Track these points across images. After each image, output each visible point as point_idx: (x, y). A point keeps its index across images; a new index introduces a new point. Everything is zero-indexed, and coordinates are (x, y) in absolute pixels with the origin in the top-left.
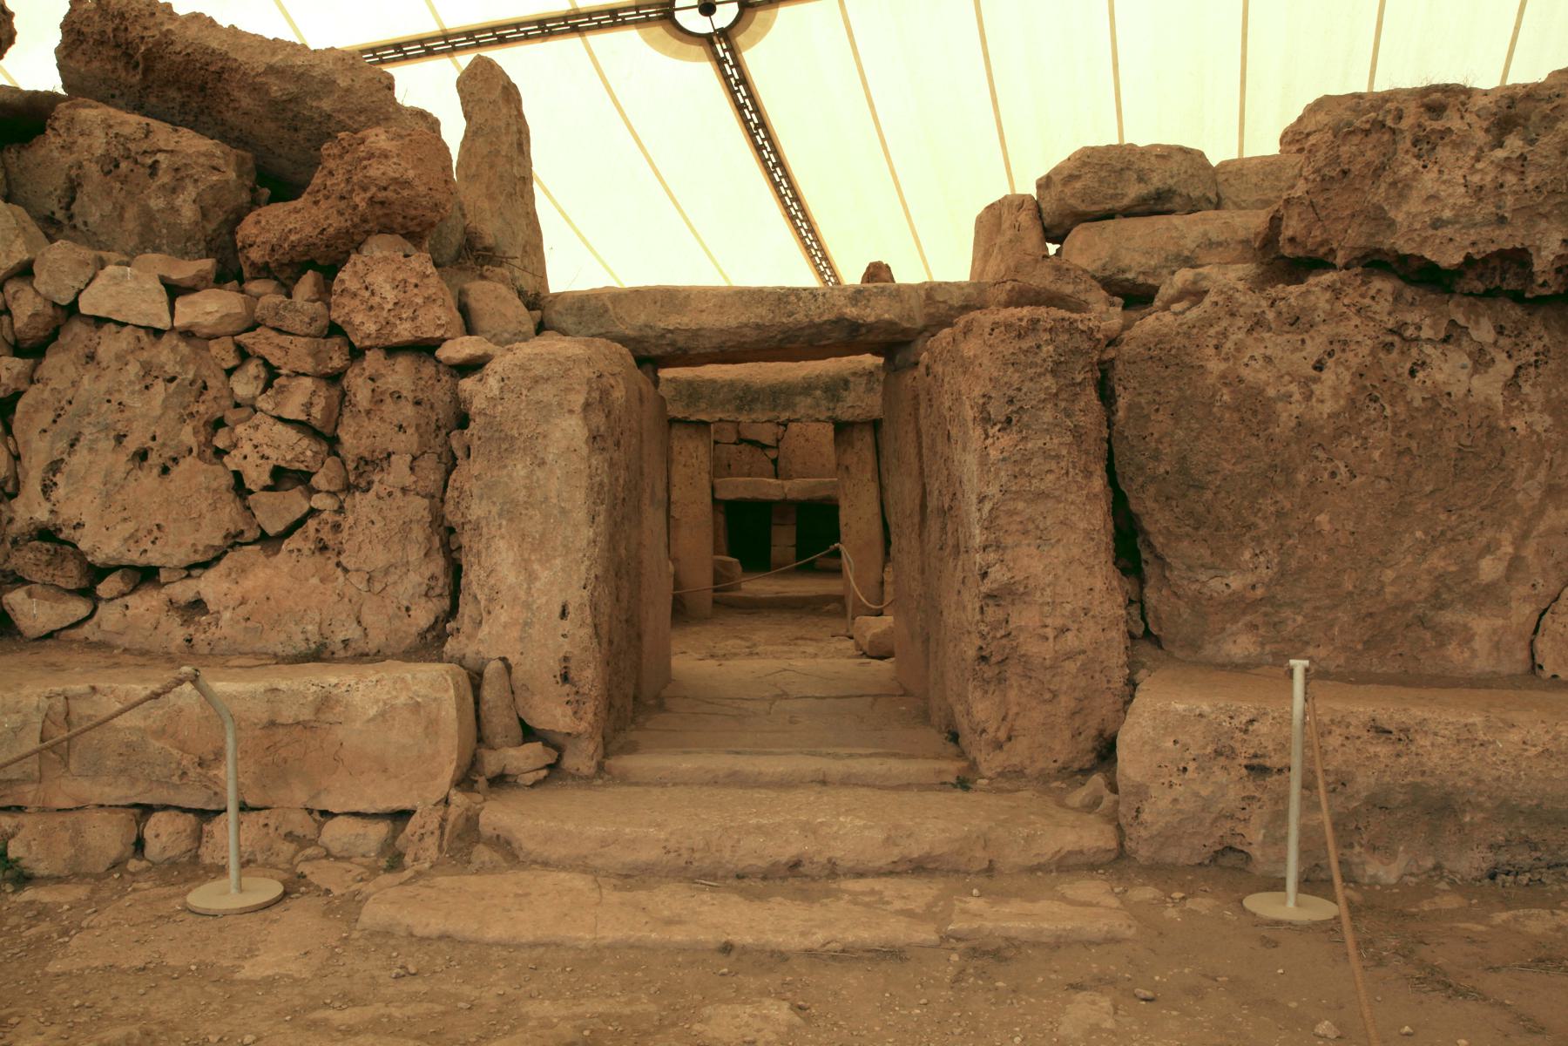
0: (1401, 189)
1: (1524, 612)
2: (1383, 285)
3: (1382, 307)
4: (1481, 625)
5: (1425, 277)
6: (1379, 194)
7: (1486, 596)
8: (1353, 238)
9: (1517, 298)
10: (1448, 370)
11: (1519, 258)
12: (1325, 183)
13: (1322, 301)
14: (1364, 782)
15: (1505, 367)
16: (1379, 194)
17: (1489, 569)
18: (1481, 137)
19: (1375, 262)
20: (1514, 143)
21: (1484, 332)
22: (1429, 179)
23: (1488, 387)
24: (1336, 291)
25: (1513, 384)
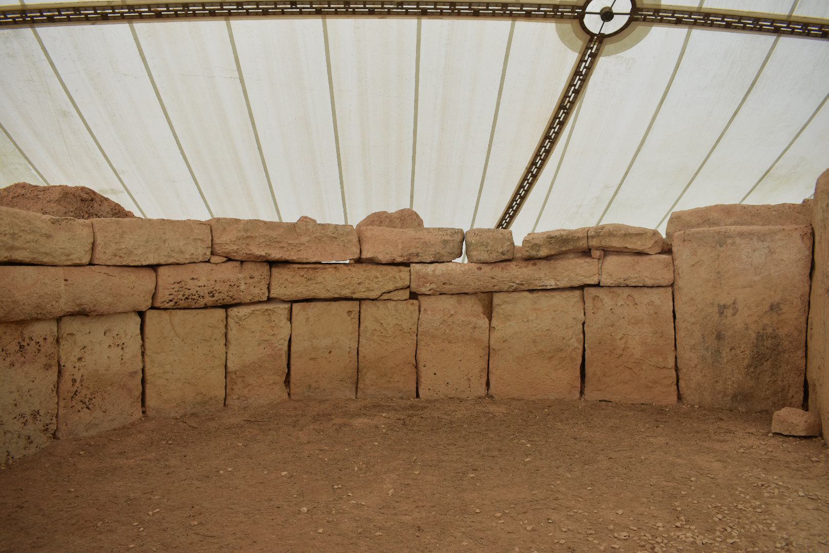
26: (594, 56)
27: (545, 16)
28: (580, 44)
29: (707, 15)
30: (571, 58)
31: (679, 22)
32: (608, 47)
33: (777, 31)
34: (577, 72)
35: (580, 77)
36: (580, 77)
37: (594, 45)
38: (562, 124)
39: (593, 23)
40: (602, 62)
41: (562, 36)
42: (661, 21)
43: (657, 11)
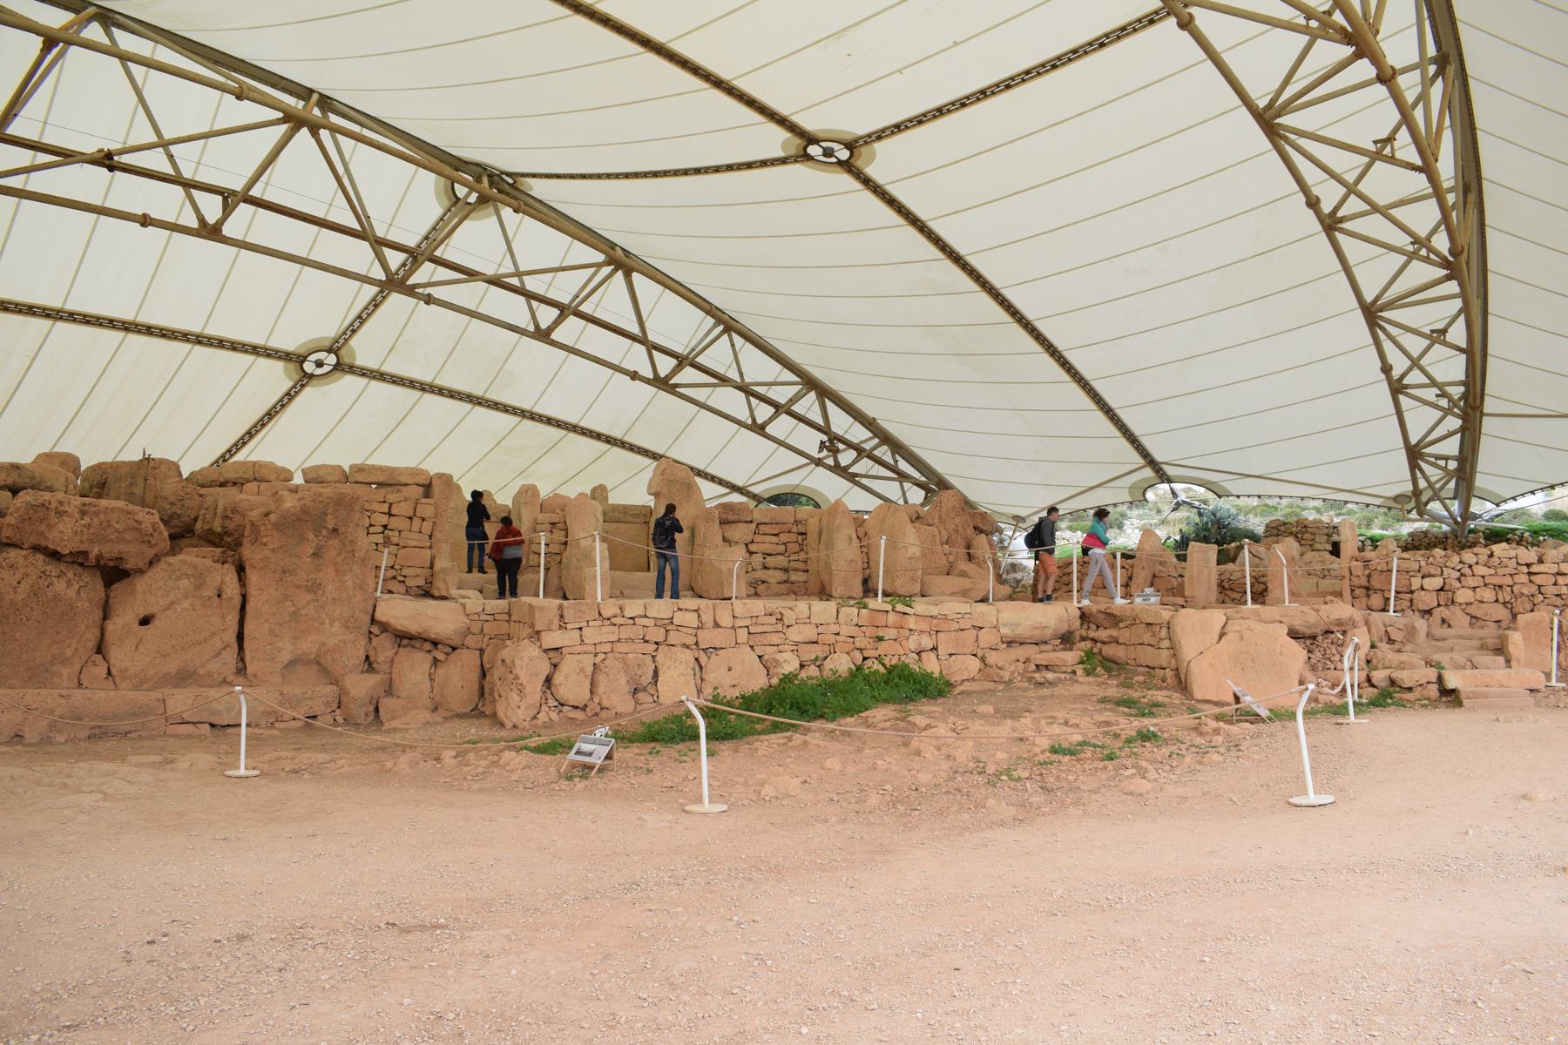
0: (50, 527)
1: (79, 666)
2: (40, 557)
3: (40, 564)
4: (65, 671)
5: (54, 555)
6: (43, 527)
7: (66, 661)
8: (33, 540)
9: (81, 565)
10: (60, 586)
11: (85, 554)
12: (23, 521)
13: (21, 560)
14: (58, 712)
15: (76, 587)
16: (43, 527)
17: (69, 652)
18: (77, 516)
19: (36, 548)
20: (87, 520)
21: (70, 575)
22: (61, 526)
23: (72, 593)
24: (25, 558)
25: (78, 592)
26: (303, 386)
27: (280, 358)
28: (296, 377)
29: (382, 374)
30: (290, 384)
31: (364, 375)
32: (314, 382)
33: (423, 390)
34: (288, 394)
35: (290, 396)
36: (290, 396)
37: (306, 379)
38: (263, 425)
39: (309, 367)
40: (307, 390)
41: (286, 371)
42: (353, 373)
43: (351, 367)
